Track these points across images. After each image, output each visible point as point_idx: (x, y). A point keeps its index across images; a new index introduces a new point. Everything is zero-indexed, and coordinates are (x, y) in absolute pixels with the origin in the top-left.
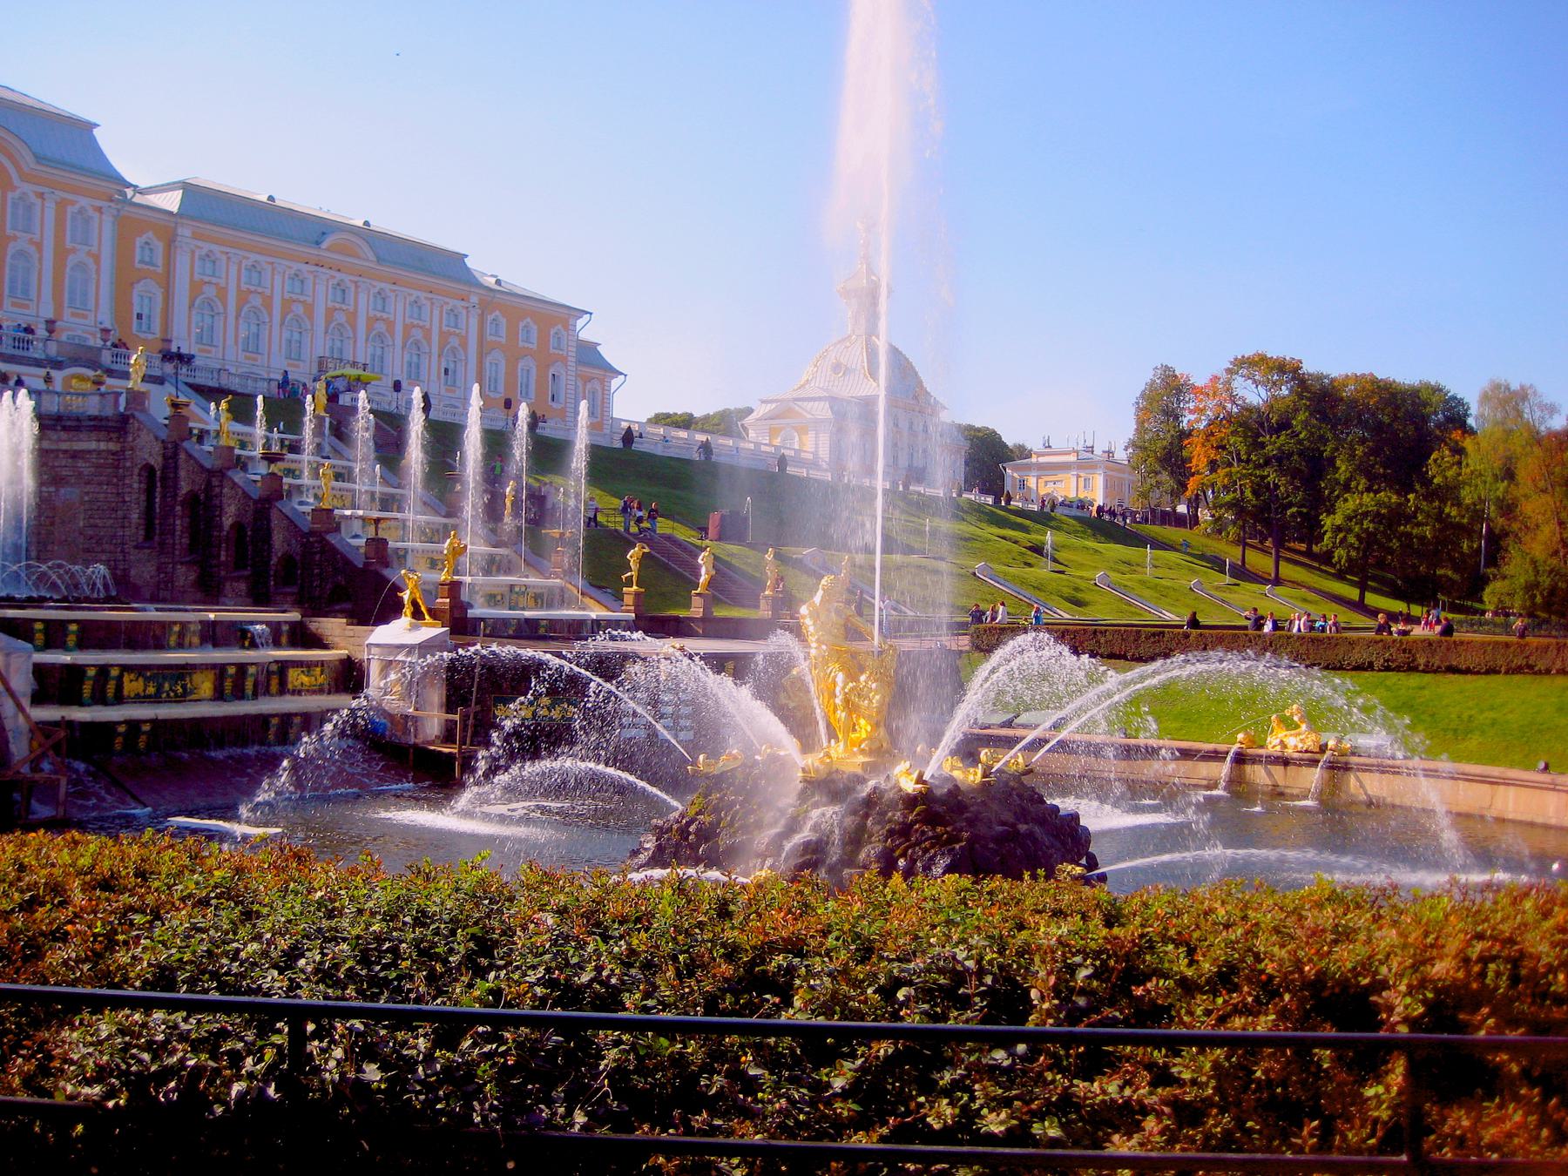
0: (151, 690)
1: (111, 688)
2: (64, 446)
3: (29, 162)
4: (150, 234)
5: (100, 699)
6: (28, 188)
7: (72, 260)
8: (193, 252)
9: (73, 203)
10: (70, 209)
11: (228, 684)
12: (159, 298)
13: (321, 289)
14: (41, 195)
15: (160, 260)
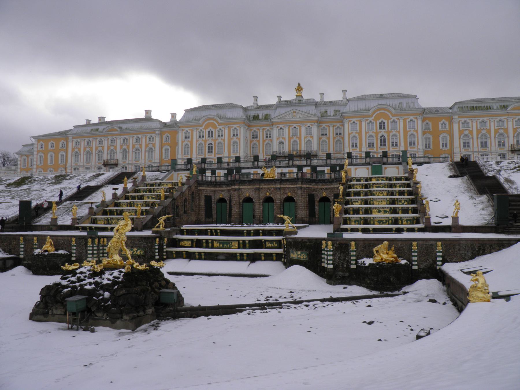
0: (221, 245)
1: (210, 245)
2: (335, 186)
3: (393, 111)
4: (444, 120)
5: (207, 247)
6: (394, 118)
7: (409, 133)
8: (459, 122)
9: (408, 118)
10: (407, 120)
11: (241, 245)
12: (448, 138)
13: (510, 123)
14: (398, 119)
15: (448, 127)
